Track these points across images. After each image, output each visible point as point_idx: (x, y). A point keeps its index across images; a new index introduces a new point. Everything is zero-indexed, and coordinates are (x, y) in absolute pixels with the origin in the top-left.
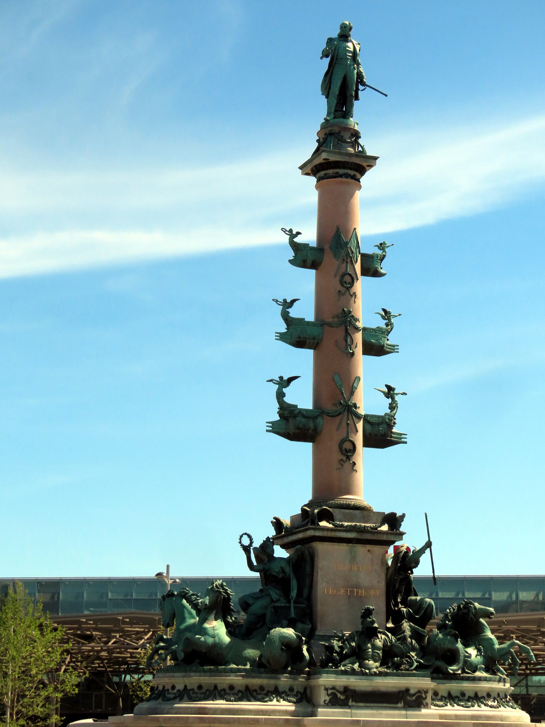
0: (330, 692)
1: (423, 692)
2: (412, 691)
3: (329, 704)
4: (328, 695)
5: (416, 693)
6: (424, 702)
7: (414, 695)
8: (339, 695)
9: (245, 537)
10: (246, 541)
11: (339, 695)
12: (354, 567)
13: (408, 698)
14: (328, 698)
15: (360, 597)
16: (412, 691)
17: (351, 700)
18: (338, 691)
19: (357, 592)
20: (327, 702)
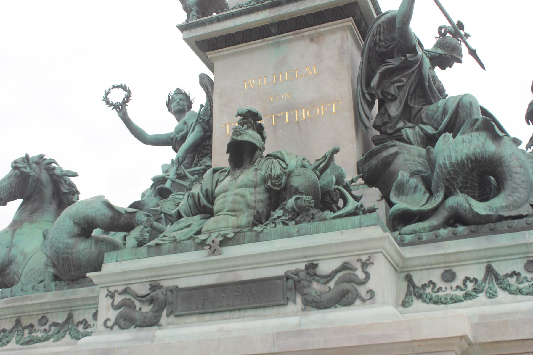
0: (118, 299)
1: (358, 266)
2: (326, 267)
3: (116, 327)
4: (116, 308)
5: (336, 272)
6: (362, 290)
7: (329, 277)
8: (138, 304)
9: (124, 94)
10: (117, 96)
11: (138, 304)
12: (283, 76)
13: (316, 286)
14: (113, 315)
15: (298, 122)
16: (326, 267)
17: (165, 313)
18: (137, 296)
19: (291, 117)
20: (110, 324)
